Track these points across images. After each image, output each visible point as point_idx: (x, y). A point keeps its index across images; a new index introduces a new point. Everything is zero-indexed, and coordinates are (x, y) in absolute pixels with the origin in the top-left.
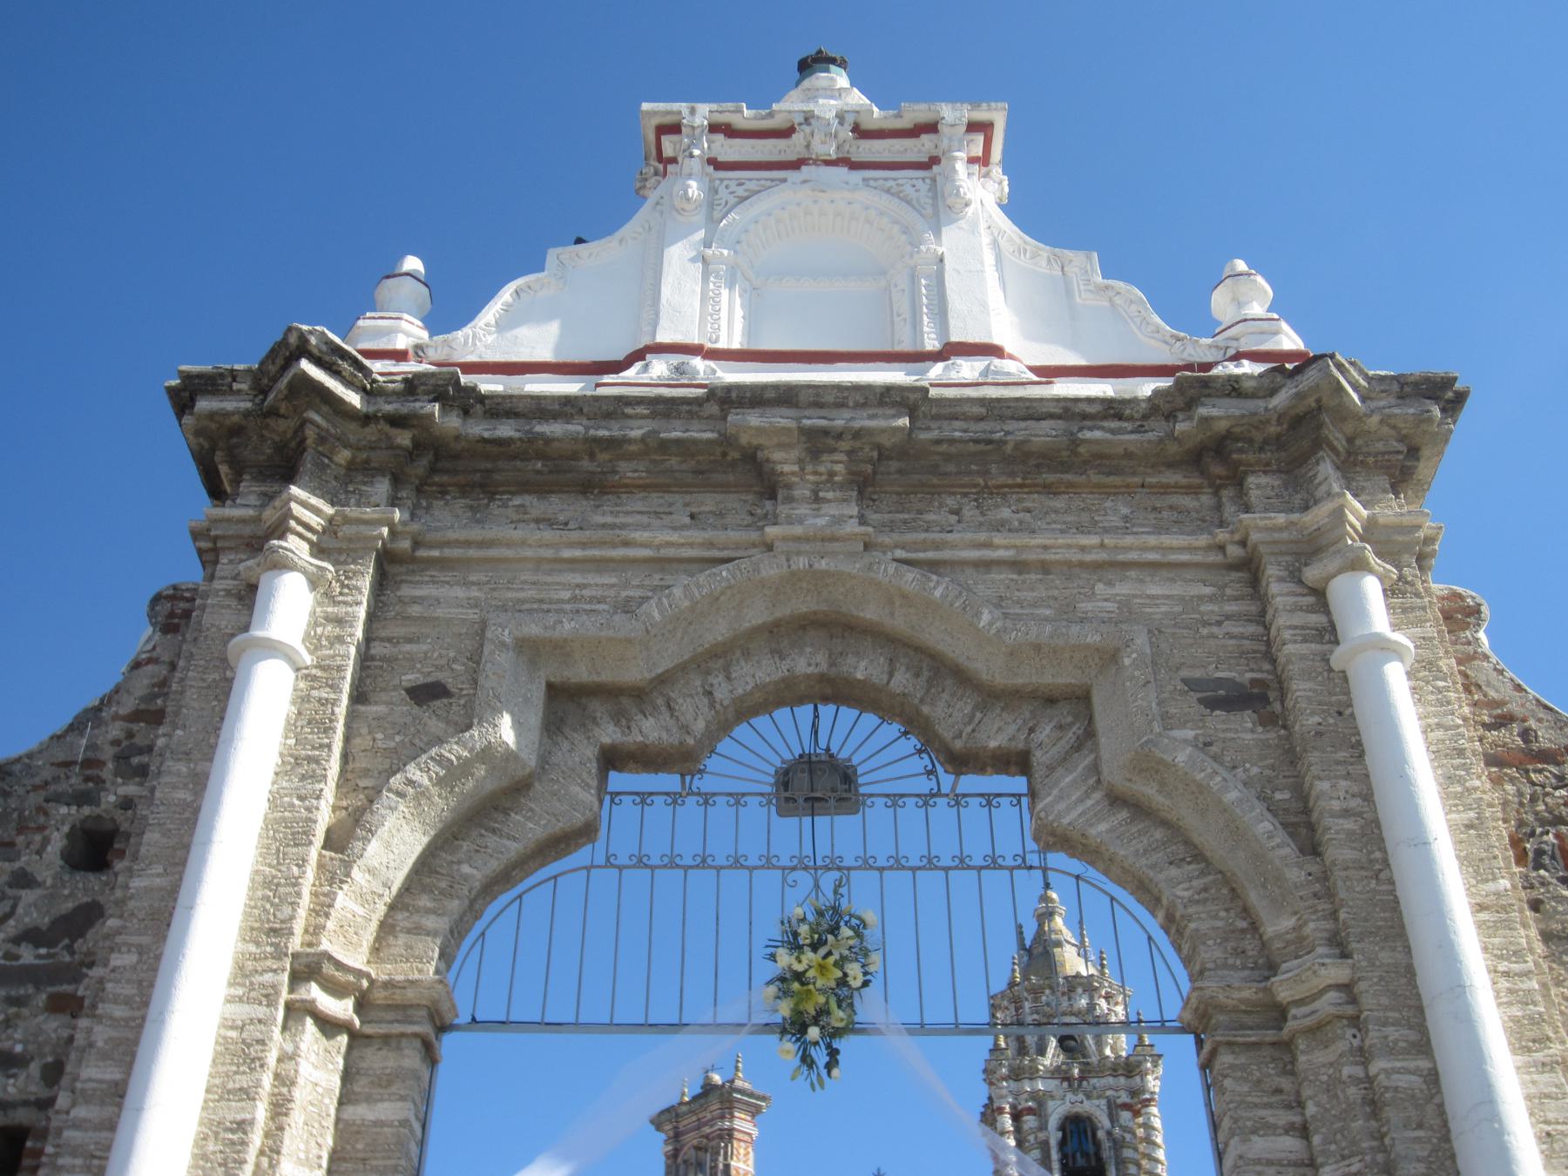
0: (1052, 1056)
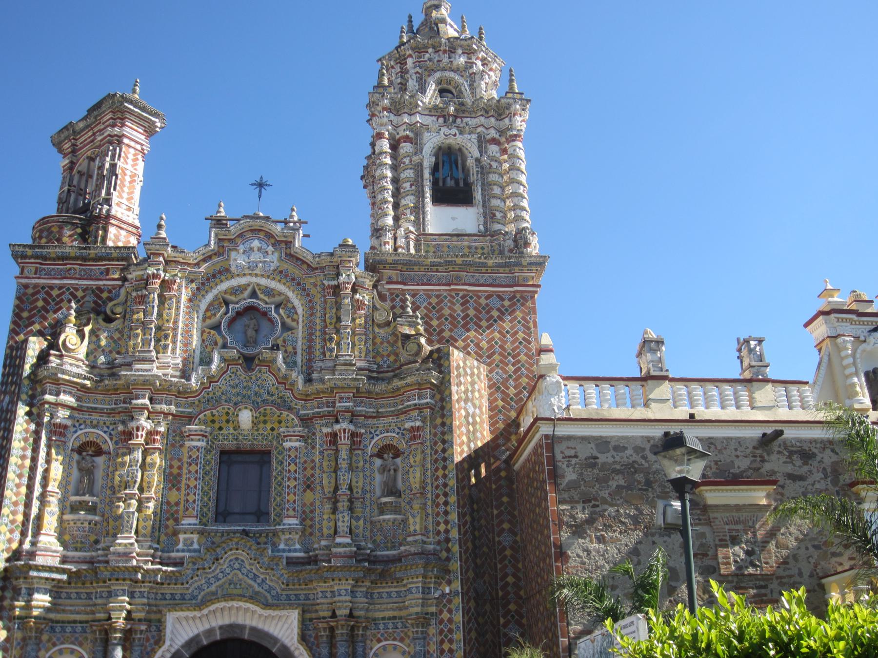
0: (430, 96)
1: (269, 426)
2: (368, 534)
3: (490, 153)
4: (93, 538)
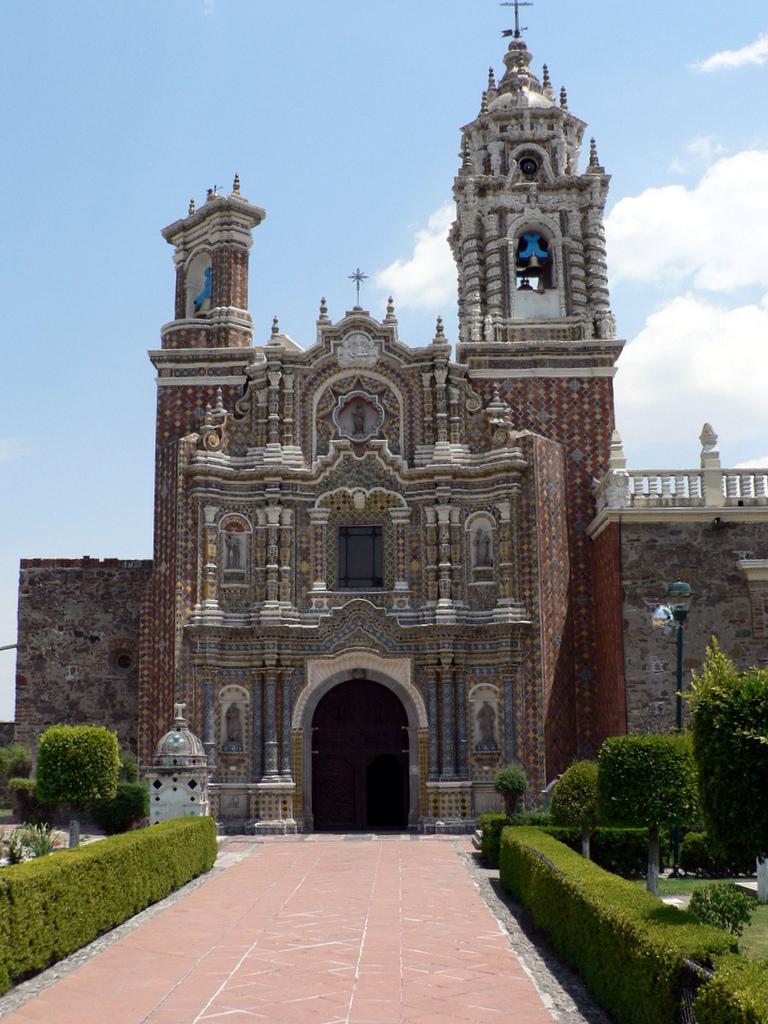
1: (379, 505)
4: (244, 602)
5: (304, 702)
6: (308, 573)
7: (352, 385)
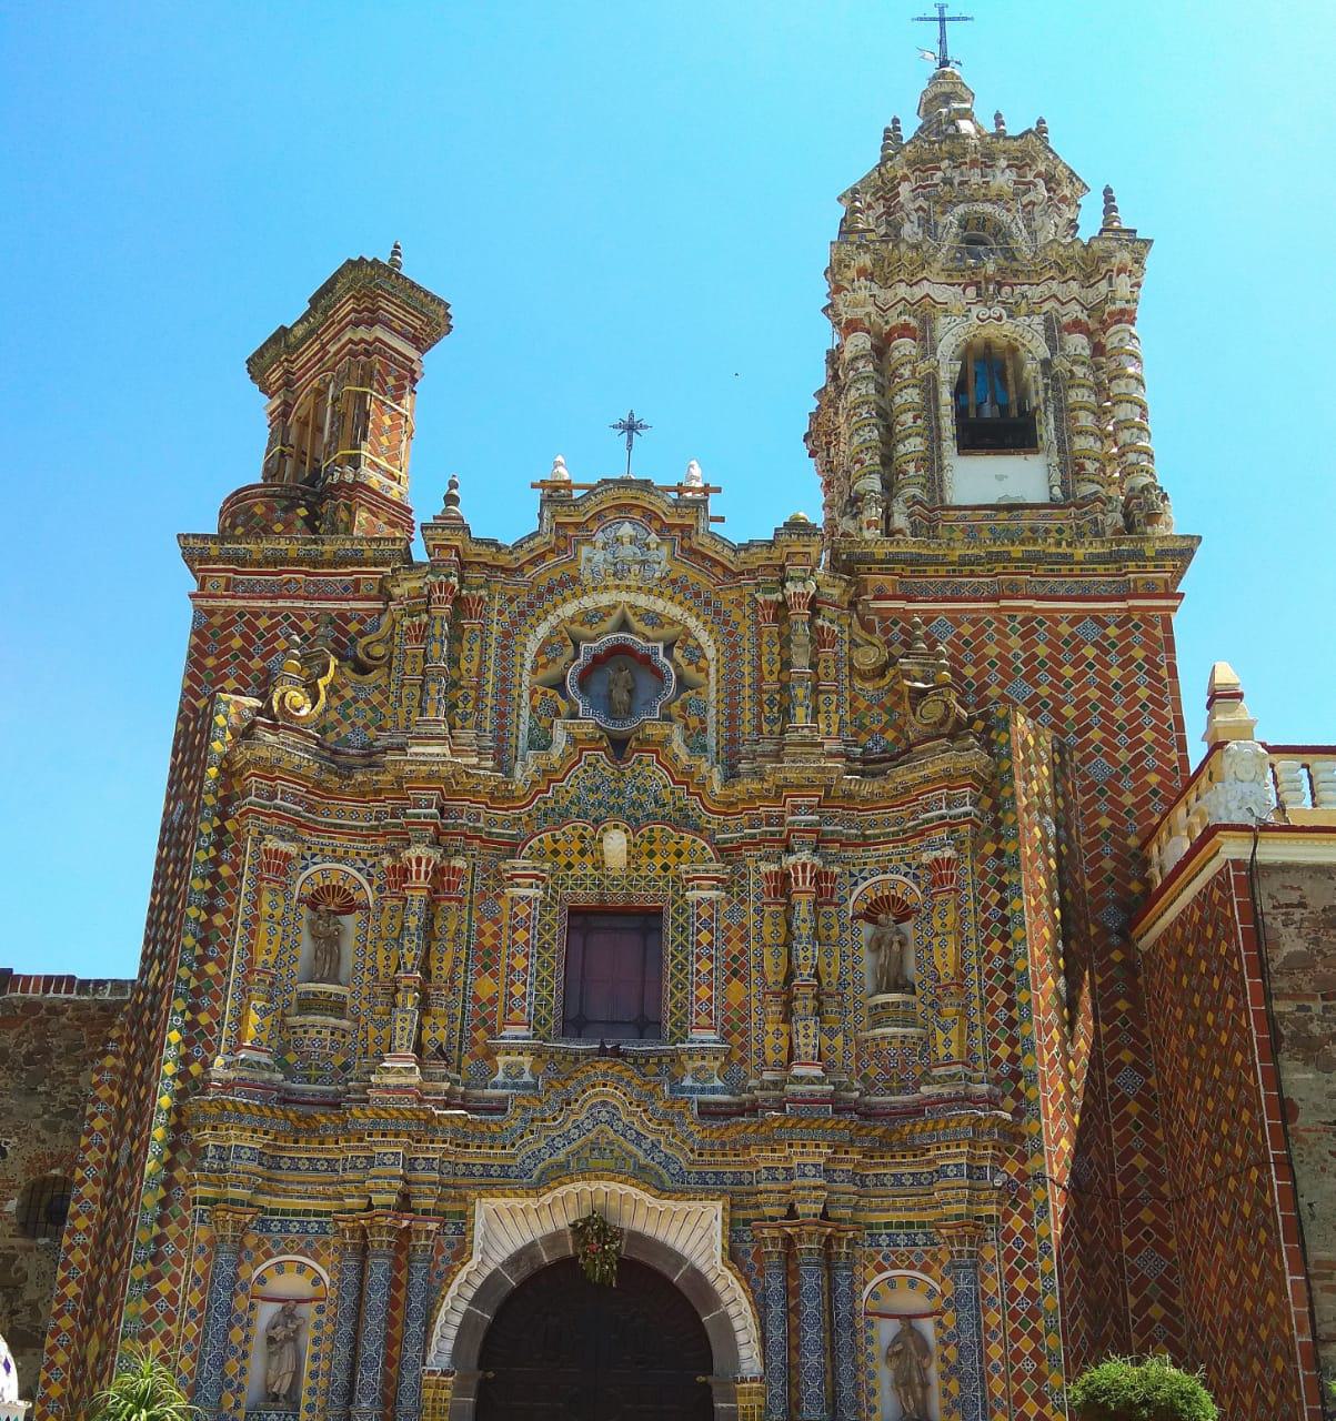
1: (658, 861)
2: (852, 1063)
3: (1070, 349)
4: (339, 1060)
5: (463, 1306)
6: (493, 1001)
7: (611, 621)
